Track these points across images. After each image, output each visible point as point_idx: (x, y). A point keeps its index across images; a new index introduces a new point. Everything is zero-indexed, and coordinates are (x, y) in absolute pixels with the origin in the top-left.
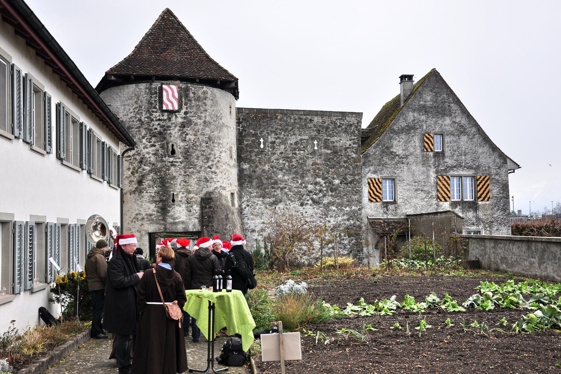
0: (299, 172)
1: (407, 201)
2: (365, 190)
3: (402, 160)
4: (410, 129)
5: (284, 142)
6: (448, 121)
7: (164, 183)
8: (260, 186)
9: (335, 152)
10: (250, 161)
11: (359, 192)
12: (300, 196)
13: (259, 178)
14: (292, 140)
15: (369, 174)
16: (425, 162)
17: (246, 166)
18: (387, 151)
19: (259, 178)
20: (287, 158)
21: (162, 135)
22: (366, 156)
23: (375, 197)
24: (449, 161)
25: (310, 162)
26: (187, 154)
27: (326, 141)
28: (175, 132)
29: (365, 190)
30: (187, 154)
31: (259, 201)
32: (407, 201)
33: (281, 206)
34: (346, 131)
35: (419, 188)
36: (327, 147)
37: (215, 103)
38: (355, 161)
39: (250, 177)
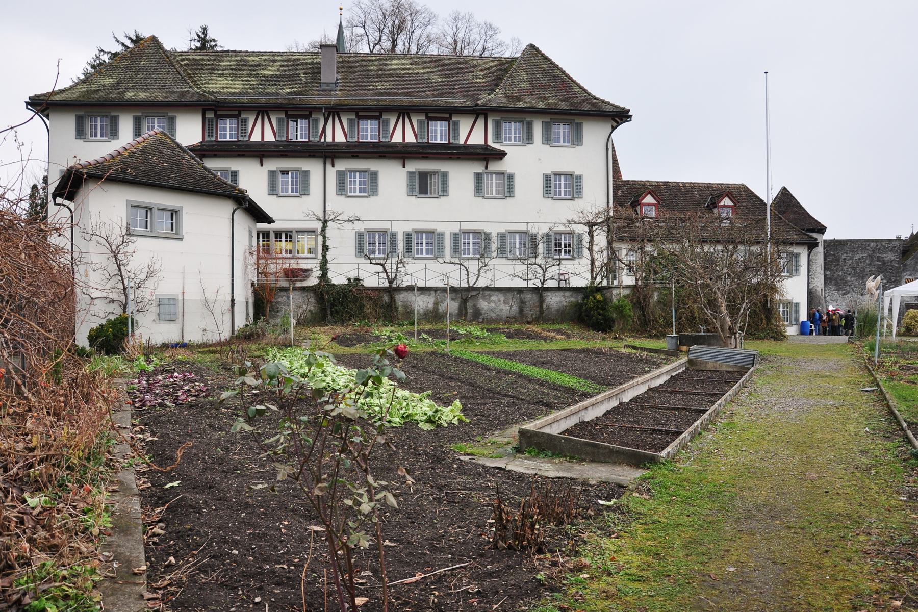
5: (851, 258)
8: (837, 284)
9: (884, 264)
10: (830, 270)
13: (836, 279)
14: (857, 257)
17: (828, 273)
19: (836, 279)
20: (853, 268)
22: (905, 266)
25: (868, 270)
27: (878, 257)
31: (836, 293)
33: (849, 295)
34: (891, 251)
36: (879, 261)
38: (897, 268)
39: (831, 279)
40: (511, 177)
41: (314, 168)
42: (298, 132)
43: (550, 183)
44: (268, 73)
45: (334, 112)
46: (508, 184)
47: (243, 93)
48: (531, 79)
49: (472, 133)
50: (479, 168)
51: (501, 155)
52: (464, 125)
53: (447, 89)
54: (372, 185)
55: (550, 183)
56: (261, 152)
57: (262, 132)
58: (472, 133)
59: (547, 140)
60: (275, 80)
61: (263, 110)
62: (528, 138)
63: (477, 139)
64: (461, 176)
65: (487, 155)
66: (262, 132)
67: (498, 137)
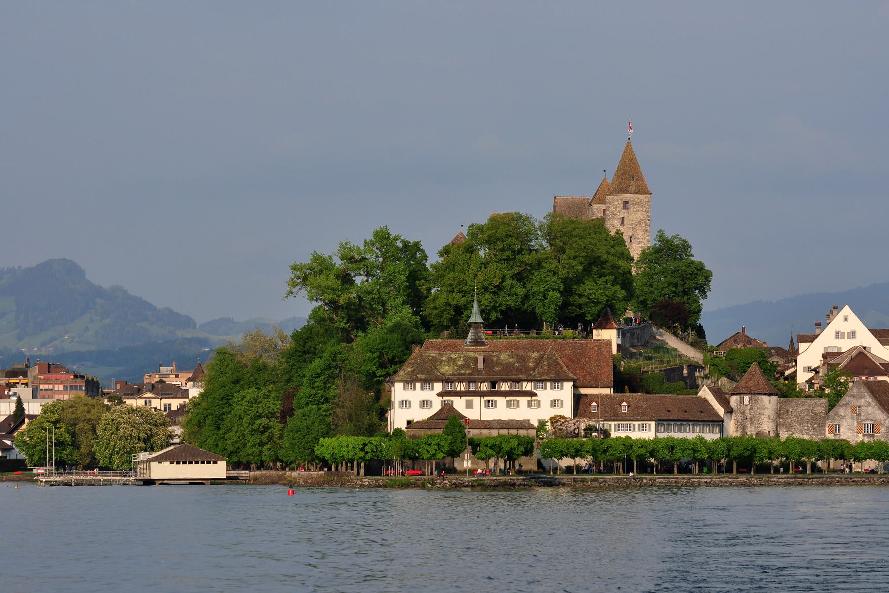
0: (801, 422)
1: (844, 434)
2: (827, 429)
3: (843, 417)
4: (846, 405)
6: (863, 400)
7: (744, 429)
11: (824, 430)
12: (801, 432)
15: (829, 423)
16: (852, 418)
18: (837, 414)
21: (743, 413)
23: (830, 432)
24: (863, 417)
26: (751, 419)
28: (748, 411)
29: (827, 429)
30: (751, 419)
32: (844, 434)
35: (850, 428)
37: (762, 401)
40: (539, 401)
41: (476, 400)
42: (472, 388)
43: (553, 403)
44: (460, 363)
45: (483, 381)
46: (539, 404)
47: (454, 374)
48: (549, 364)
49: (527, 387)
50: (529, 398)
51: (536, 395)
52: (525, 384)
53: (519, 370)
54: (495, 404)
55: (553, 403)
56: (460, 394)
57: (461, 387)
58: (527, 387)
59: (551, 388)
60: (462, 367)
61: (461, 381)
62: (546, 388)
63: (529, 389)
64: (523, 401)
65: (532, 394)
66: (461, 387)
67: (535, 388)
